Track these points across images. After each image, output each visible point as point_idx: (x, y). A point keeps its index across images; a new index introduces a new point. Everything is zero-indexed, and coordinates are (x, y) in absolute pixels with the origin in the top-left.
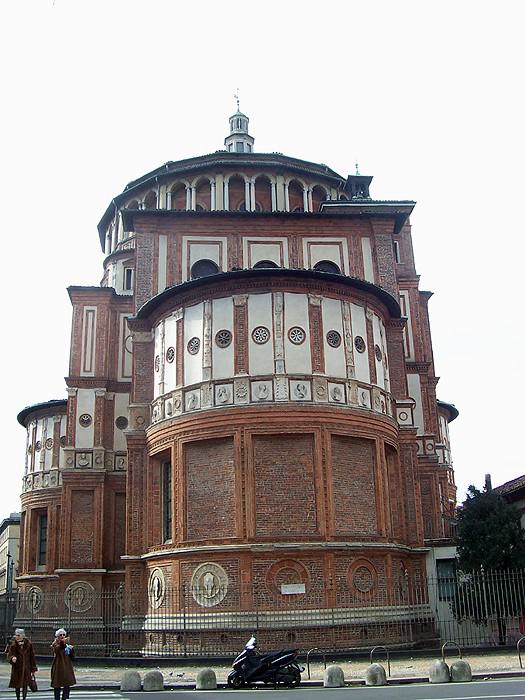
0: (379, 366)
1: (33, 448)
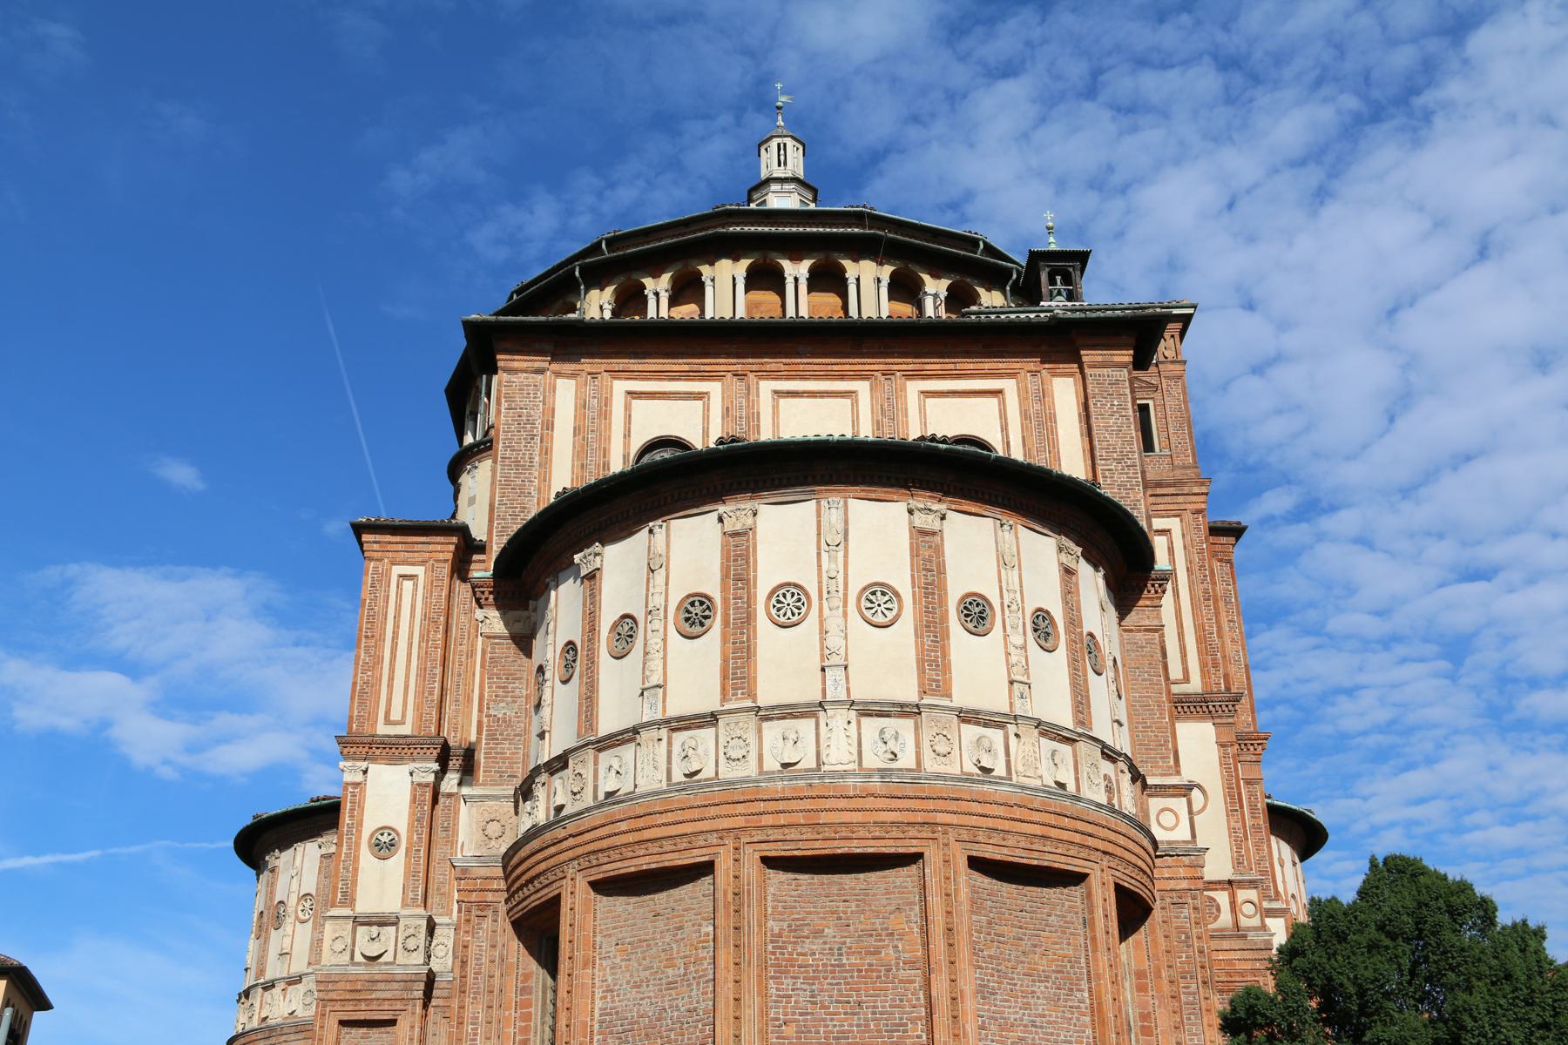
0: (1100, 688)
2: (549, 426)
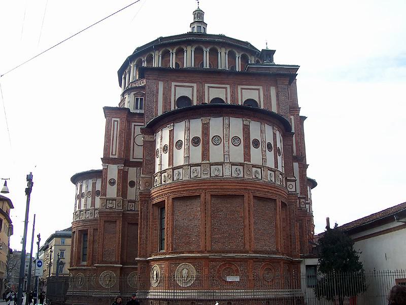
0: (279, 158)
1: (79, 197)
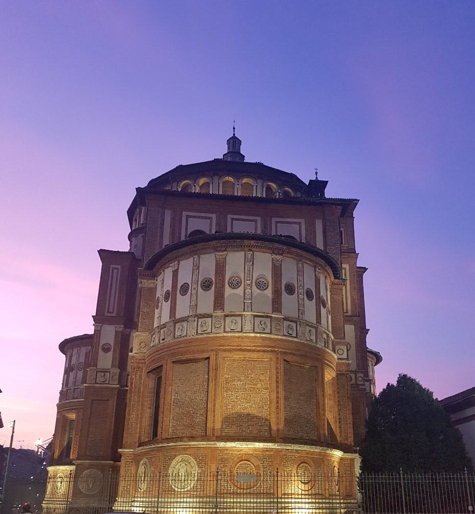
2: (162, 224)
